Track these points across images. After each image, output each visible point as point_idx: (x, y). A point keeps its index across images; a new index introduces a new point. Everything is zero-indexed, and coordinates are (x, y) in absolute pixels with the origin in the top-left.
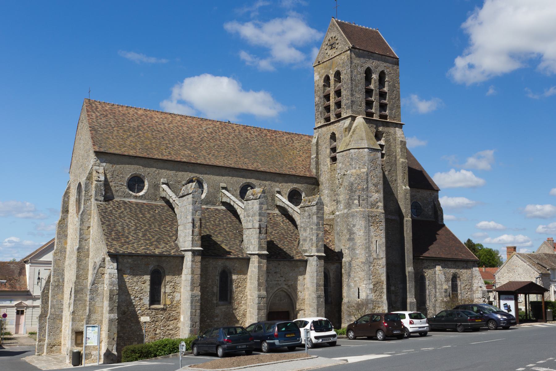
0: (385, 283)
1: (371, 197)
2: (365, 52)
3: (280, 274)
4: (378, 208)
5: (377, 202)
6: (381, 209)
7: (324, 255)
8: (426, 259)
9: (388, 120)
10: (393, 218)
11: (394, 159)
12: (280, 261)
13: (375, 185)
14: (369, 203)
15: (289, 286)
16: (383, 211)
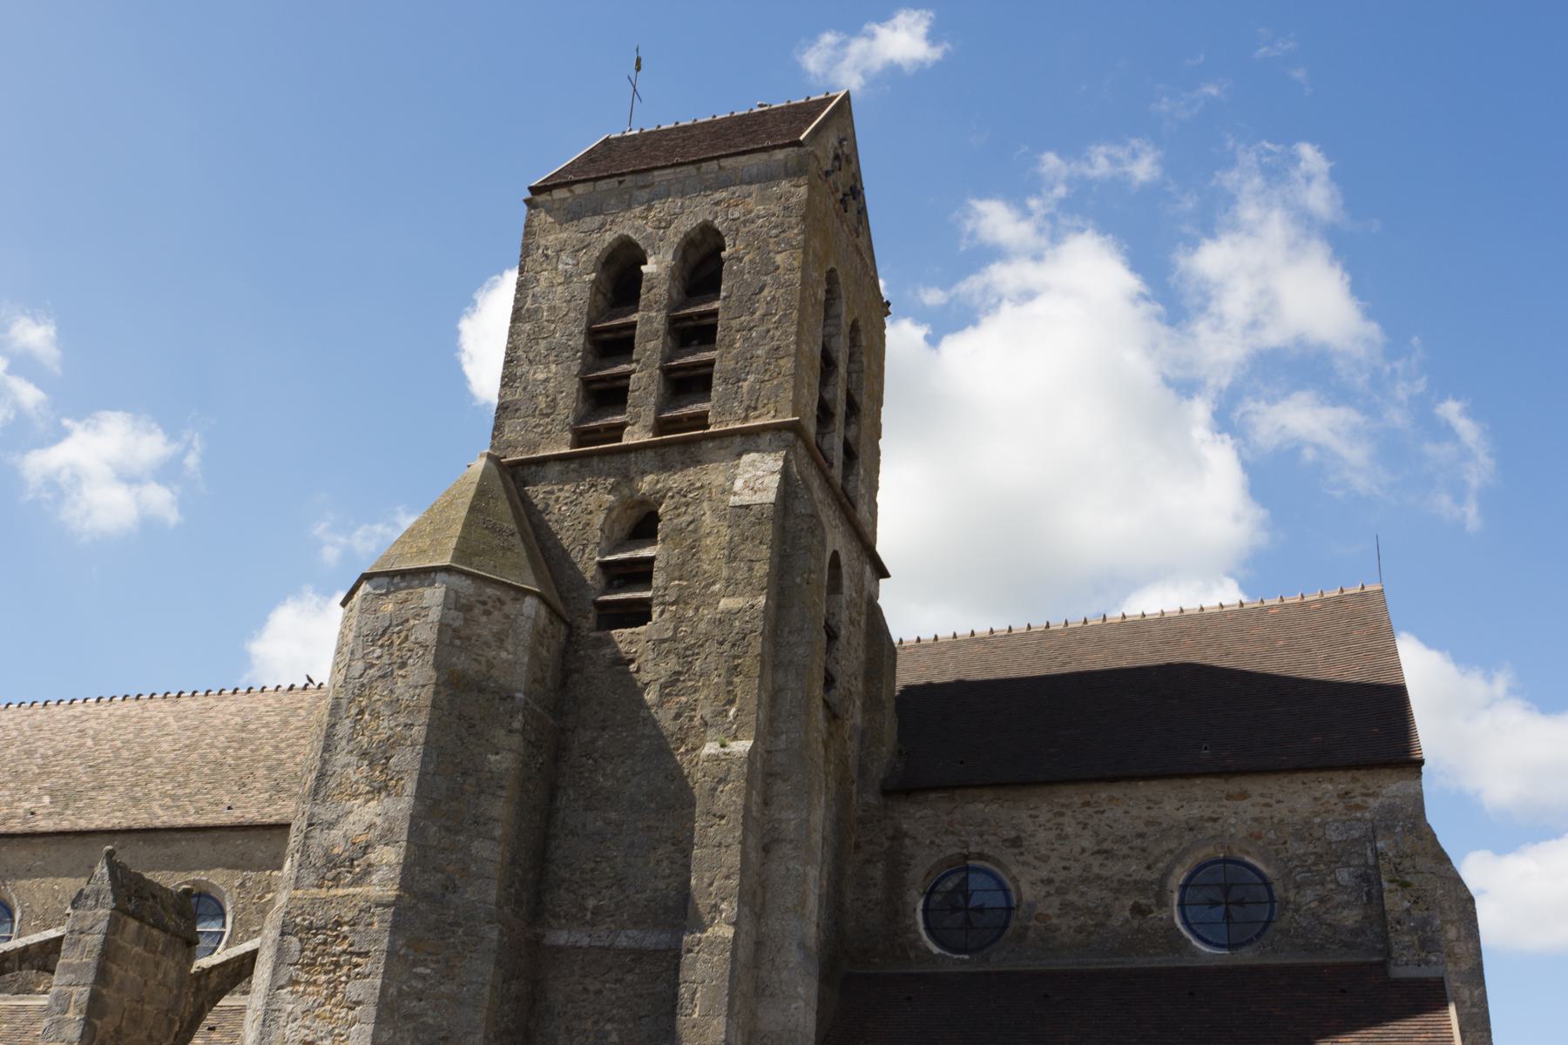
1: (331, 825)
2: (602, 185)
4: (369, 869)
5: (367, 848)
14: (316, 852)
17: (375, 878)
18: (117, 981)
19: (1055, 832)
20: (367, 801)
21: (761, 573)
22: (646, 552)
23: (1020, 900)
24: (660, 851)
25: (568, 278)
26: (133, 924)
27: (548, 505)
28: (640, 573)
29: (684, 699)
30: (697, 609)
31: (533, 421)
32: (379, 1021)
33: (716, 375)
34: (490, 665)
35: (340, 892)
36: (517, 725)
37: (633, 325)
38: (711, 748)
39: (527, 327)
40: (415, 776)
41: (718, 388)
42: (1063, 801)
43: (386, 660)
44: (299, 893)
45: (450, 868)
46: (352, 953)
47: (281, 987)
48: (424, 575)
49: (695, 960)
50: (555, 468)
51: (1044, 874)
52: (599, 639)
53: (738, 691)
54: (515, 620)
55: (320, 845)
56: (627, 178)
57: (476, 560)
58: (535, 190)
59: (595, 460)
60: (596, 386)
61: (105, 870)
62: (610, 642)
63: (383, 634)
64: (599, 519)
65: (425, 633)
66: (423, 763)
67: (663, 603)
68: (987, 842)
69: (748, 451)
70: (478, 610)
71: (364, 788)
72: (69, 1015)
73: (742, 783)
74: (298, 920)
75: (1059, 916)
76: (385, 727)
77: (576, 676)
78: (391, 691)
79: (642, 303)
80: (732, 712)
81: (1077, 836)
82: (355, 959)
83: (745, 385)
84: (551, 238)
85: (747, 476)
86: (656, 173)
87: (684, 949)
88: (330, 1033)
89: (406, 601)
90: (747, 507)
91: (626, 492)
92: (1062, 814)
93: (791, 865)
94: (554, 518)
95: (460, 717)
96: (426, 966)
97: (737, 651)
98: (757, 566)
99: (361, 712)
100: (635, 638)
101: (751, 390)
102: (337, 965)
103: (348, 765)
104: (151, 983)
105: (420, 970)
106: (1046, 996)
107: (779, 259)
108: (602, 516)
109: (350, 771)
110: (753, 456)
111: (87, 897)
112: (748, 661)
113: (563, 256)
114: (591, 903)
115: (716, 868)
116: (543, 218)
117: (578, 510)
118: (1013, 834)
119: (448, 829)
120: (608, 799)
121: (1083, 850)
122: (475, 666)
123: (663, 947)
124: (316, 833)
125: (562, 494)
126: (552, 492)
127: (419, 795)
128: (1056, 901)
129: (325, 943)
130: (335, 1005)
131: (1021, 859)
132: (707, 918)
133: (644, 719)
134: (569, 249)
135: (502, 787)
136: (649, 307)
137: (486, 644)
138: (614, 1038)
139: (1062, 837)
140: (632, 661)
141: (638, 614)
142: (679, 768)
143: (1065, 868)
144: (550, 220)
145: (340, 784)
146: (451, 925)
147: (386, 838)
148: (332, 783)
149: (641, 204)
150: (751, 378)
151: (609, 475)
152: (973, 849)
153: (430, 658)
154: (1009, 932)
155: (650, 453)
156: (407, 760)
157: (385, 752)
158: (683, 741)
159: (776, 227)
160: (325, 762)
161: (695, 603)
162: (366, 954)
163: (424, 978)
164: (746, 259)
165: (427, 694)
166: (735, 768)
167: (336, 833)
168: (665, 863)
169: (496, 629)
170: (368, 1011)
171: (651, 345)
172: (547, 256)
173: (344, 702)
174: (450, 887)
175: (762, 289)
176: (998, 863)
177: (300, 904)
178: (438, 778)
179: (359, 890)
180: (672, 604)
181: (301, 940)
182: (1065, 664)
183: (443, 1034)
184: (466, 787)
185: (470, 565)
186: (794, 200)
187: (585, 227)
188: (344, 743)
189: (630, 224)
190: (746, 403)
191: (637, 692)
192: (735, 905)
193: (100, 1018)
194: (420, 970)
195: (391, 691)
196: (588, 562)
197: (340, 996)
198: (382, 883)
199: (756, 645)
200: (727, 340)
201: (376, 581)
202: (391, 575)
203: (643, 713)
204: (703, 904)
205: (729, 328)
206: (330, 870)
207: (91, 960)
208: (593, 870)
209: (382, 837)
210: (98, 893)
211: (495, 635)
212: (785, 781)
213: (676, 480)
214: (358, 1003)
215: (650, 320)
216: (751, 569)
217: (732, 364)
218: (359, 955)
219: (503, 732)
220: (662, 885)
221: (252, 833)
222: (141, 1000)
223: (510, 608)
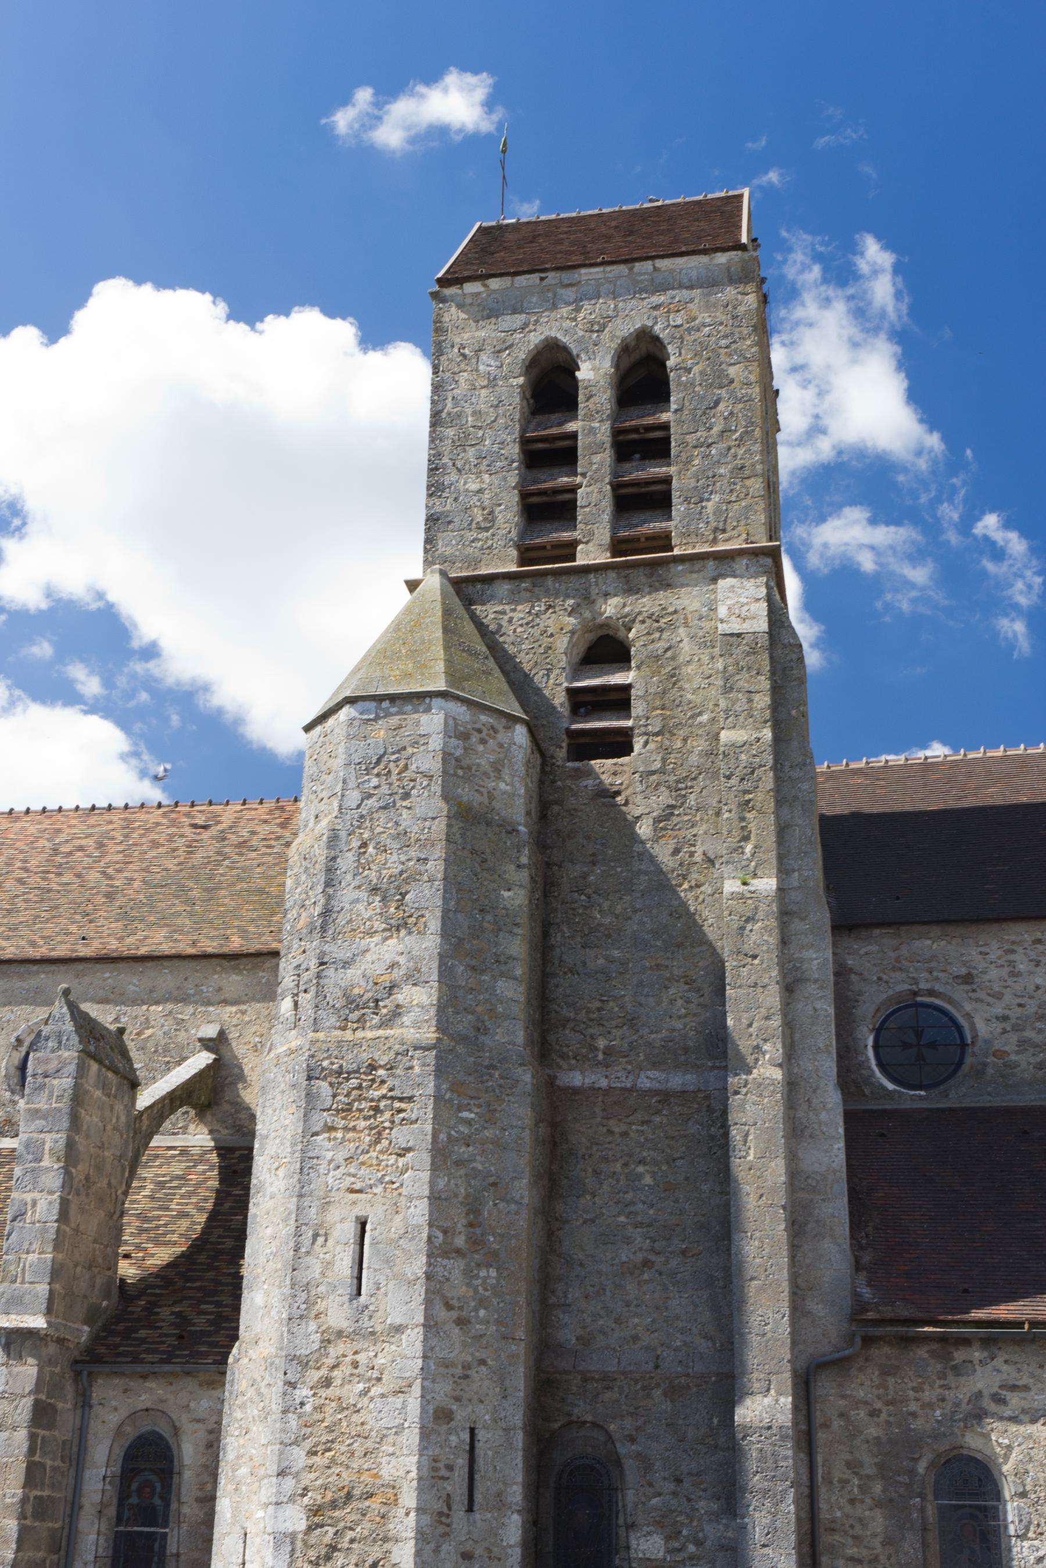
0: (409, 1498)
1: (346, 964)
2: (522, 280)
4: (397, 1012)
5: (392, 988)
6: (417, 1025)
7: (38, 1322)
8: (987, 1342)
9: (676, 552)
10: (676, 1081)
11: (700, 745)
13: (390, 892)
14: (334, 995)
16: (429, 1034)
17: (406, 1020)
18: (85, 1127)
19: (1007, 970)
20: (386, 939)
21: (762, 705)
22: (618, 679)
23: (975, 1036)
24: (672, 991)
25: (492, 382)
26: (94, 1067)
27: (500, 626)
28: (618, 700)
29: (683, 833)
30: (685, 740)
31: (470, 535)
32: (434, 1168)
33: (675, 494)
34: (491, 797)
35: (369, 1034)
36: (524, 860)
37: (574, 436)
38: (731, 886)
39: (450, 432)
40: (439, 914)
41: (679, 508)
42: (1013, 938)
43: (385, 789)
44: (321, 1035)
45: (479, 1009)
46: (392, 1098)
47: (316, 1134)
48: (419, 699)
49: (744, 1102)
50: (504, 588)
51: (999, 1011)
52: (577, 769)
53: (752, 827)
54: (508, 749)
55: (336, 985)
56: (551, 275)
57: (466, 684)
58: (443, 282)
59: (550, 580)
60: (534, 500)
61: (65, 1010)
62: (590, 773)
63: (378, 762)
64: (562, 643)
65: (428, 760)
66: (444, 898)
67: (645, 734)
68: (937, 979)
69: (724, 576)
70: (475, 738)
71: (378, 925)
72: (46, 1163)
73: (773, 923)
74: (325, 1063)
75: (1017, 1053)
76: (394, 863)
77: (556, 808)
78: (397, 823)
79: (581, 413)
80: (749, 848)
81: (1031, 973)
82: (397, 1105)
83: (710, 504)
84: (466, 336)
85: (729, 602)
86: (583, 271)
87: (731, 1090)
88: (381, 1181)
89: (400, 727)
90: (739, 635)
91: (587, 614)
92: (1013, 951)
93: (819, 1005)
94: (509, 640)
95: (473, 852)
96: (471, 1111)
97: (747, 785)
98: (757, 697)
99: (364, 845)
100: (619, 769)
101: (718, 512)
102: (377, 1110)
103: (357, 901)
104: (109, 1127)
105: (465, 1114)
106: (1025, 1132)
107: (732, 371)
108: (566, 640)
109: (360, 907)
110: (730, 581)
111: (47, 1039)
112: (760, 796)
113: (484, 357)
114: (601, 1043)
115: (753, 1012)
116: (453, 314)
117: (536, 632)
118: (964, 971)
119: (473, 968)
120: (609, 936)
121: (1038, 988)
122: (478, 798)
123: (692, 1088)
124: (330, 972)
125: (516, 616)
126: (504, 613)
127: (447, 931)
128: (1013, 1038)
129: (360, 1087)
130: (381, 1152)
131: (973, 995)
132: (750, 1060)
133: (639, 854)
134: (489, 350)
135: (517, 925)
136: (589, 417)
137: (485, 774)
138: (648, 1180)
139: (1015, 974)
140: (618, 793)
141: (618, 744)
142: (684, 905)
143: (1020, 1005)
144: (463, 316)
145: (350, 921)
146: (487, 1067)
147: (414, 978)
148: (342, 919)
149: (568, 304)
150: (715, 498)
151: (567, 596)
152: (923, 986)
153: (436, 788)
154: (965, 1068)
155: (612, 574)
156: (427, 897)
157: (398, 888)
158: (684, 877)
159: (726, 337)
160: (329, 898)
161: (682, 733)
162: (410, 1099)
163: (469, 1122)
164: (696, 370)
165: (439, 827)
166: (763, 907)
167: (353, 974)
168: (680, 1002)
169: (492, 758)
170: (421, 1158)
171: (597, 458)
172: (464, 356)
173: (343, 834)
174: (480, 1028)
175: (717, 403)
176: (950, 1000)
177: (324, 1047)
178: (459, 916)
179: (389, 1032)
180: (657, 734)
181: (331, 1084)
182: (960, 798)
183: (492, 1180)
184: (485, 924)
185: (463, 690)
186: (742, 309)
187: (505, 326)
188: (349, 877)
189: (556, 326)
190: (714, 524)
191: (626, 827)
192: (779, 1046)
193: (75, 1167)
194: (465, 1114)
195: (397, 823)
196: (556, 688)
197: (385, 1143)
198: (417, 1025)
199: (768, 781)
200: (684, 456)
201: (360, 705)
202: (379, 699)
203: (638, 848)
204: (744, 1045)
205: (683, 443)
206: (352, 1011)
207: (64, 1105)
208: (599, 1009)
209: (408, 977)
210: (59, 1035)
211: (493, 764)
212: (802, 919)
213: (647, 603)
214: (408, 1150)
215: (592, 431)
216: (750, 701)
217: (693, 483)
218: (401, 1099)
219: (513, 867)
220: (678, 1025)
221: (122, 965)
222: (101, 1147)
223: (502, 736)
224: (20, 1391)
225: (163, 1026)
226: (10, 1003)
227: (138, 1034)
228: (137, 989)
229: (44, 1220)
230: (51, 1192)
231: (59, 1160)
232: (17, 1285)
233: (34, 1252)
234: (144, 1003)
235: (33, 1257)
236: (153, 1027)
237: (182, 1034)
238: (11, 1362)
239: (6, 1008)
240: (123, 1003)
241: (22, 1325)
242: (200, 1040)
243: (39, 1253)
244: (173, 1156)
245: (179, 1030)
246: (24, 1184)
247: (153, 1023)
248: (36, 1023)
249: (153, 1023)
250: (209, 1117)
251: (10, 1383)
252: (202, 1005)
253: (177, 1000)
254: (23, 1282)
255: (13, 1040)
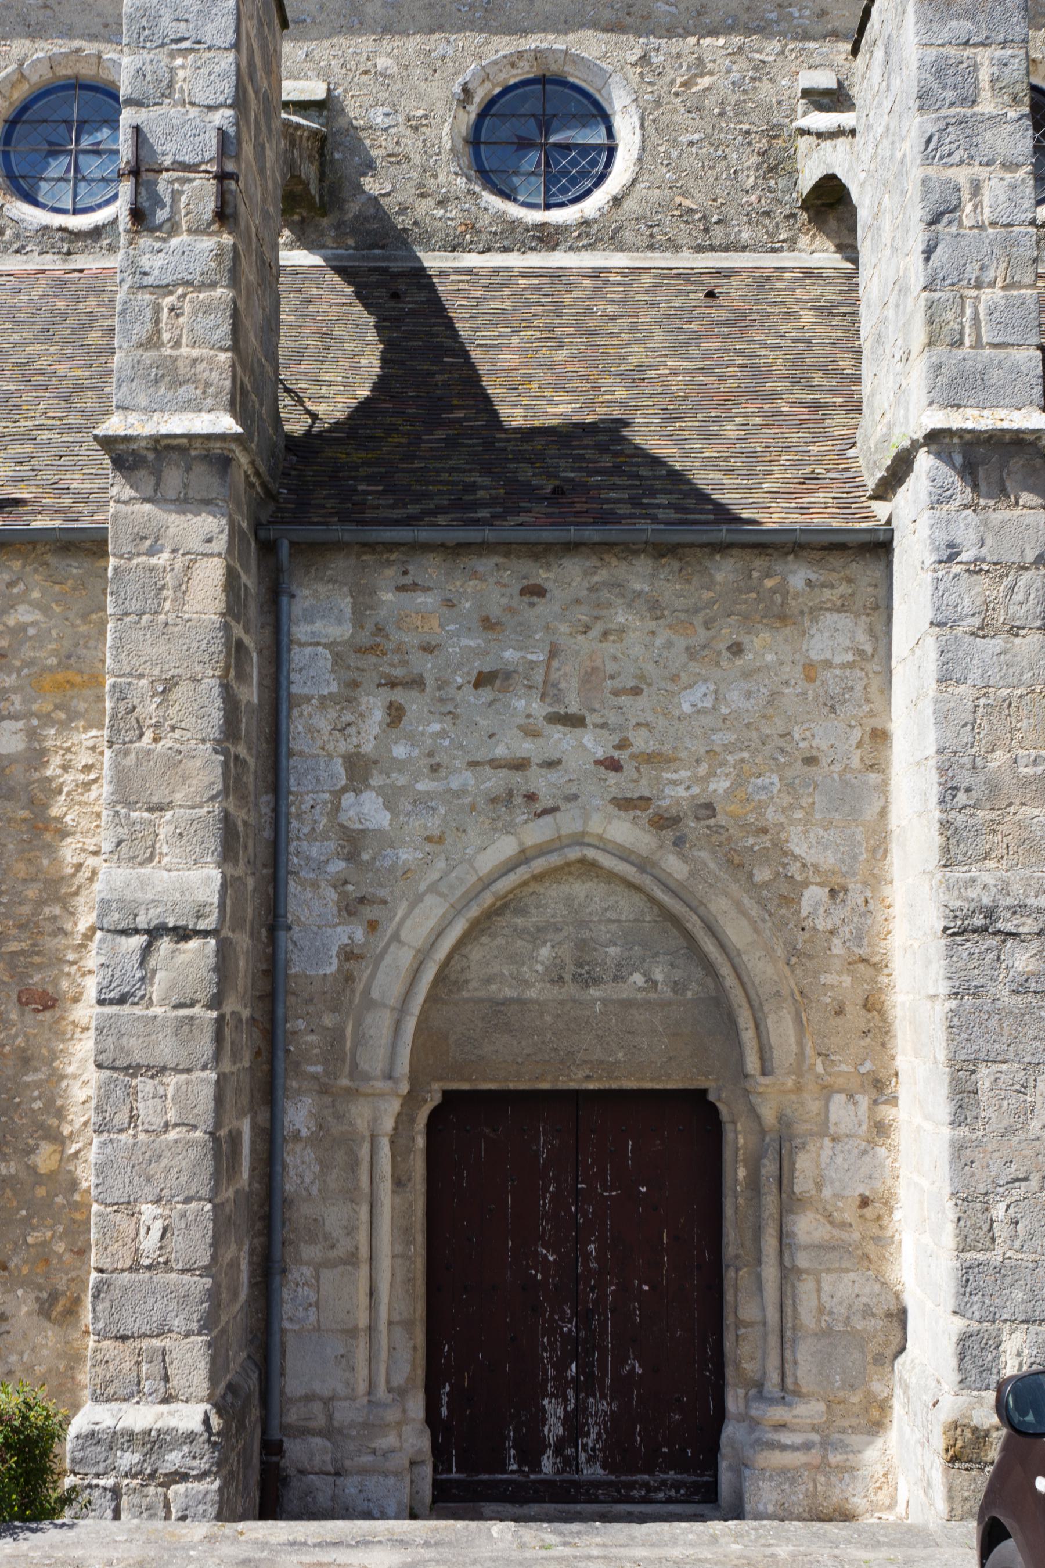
3: (549, 691)
12: (541, 552)
15: (665, 822)
72: (987, 106)
224: (1015, 558)
225: (729, 71)
226: (441, 28)
227: (684, 84)
228: (673, 9)
229: (1005, 220)
230: (1010, 166)
231: (1015, 100)
232: (965, 351)
233: (992, 285)
234: (687, 33)
235: (987, 296)
236: (711, 73)
237: (765, 86)
238: (982, 502)
239: (436, 36)
240: (652, 32)
241: (1006, 425)
242: (806, 93)
243: (1003, 288)
244: (797, 279)
245: (760, 79)
246: (945, 149)
247: (710, 66)
248: (495, 63)
249: (710, 66)
250: (833, 224)
251: (989, 542)
252: (795, 39)
253: (749, 31)
254: (978, 345)
255: (457, 89)
